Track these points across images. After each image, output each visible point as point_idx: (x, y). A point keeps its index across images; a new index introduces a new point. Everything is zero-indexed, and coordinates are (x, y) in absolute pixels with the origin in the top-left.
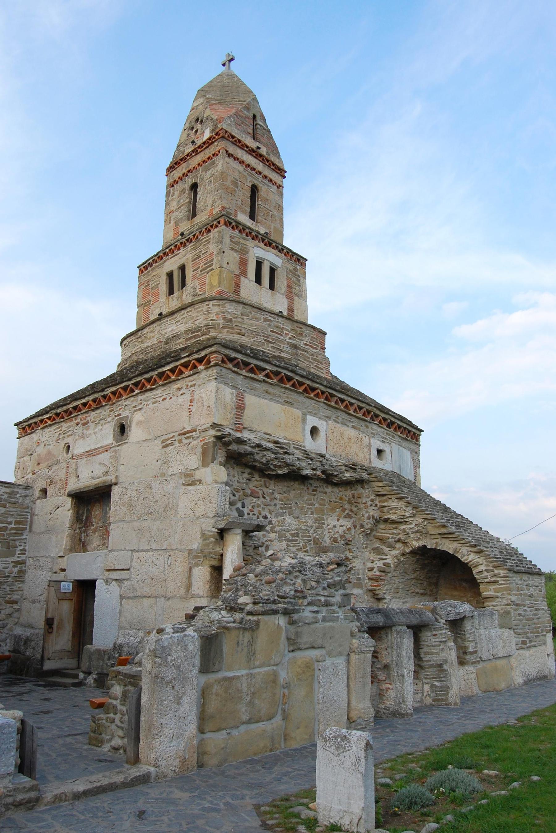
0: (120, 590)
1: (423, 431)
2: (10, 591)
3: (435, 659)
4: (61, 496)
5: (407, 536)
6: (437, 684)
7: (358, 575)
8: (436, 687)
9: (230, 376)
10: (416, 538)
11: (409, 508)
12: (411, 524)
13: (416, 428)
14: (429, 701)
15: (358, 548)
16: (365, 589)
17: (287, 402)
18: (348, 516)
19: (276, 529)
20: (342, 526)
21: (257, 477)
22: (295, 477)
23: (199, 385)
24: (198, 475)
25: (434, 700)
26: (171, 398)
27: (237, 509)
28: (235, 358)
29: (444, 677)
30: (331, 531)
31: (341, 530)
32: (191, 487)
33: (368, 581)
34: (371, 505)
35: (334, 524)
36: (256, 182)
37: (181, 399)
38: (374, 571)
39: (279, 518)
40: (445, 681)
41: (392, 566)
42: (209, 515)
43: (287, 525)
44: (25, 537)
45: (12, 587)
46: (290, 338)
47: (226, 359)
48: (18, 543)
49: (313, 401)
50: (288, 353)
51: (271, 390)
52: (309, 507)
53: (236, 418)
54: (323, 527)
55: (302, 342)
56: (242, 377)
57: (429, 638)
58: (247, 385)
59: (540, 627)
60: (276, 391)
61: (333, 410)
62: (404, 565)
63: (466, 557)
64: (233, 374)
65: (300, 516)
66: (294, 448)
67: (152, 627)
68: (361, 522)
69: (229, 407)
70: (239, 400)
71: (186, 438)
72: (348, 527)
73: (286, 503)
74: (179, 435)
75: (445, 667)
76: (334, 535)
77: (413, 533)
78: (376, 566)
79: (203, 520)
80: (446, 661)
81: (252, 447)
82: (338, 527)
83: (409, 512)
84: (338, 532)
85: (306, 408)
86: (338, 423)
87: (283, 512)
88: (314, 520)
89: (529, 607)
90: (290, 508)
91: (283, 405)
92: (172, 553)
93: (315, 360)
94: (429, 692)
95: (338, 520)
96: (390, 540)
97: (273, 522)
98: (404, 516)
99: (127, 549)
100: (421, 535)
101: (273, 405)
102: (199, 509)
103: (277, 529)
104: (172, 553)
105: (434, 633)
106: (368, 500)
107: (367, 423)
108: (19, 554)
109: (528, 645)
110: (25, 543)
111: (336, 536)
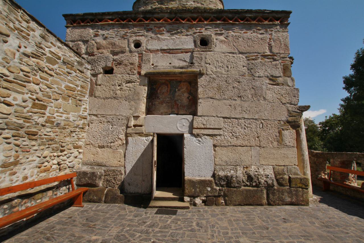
0: (213, 142)
2: (77, 138)
4: (134, 75)
23: (276, 32)
24: (280, 80)
26: (252, 33)
32: (275, 86)
37: (260, 36)
42: (293, 103)
44: (86, 99)
45: (79, 136)
48: (83, 103)
67: (249, 164)
71: (268, 58)
74: (262, 56)
79: (288, 105)
92: (263, 121)
99: (219, 116)
102: (284, 99)
104: (263, 121)
108: (83, 111)
110: (86, 103)
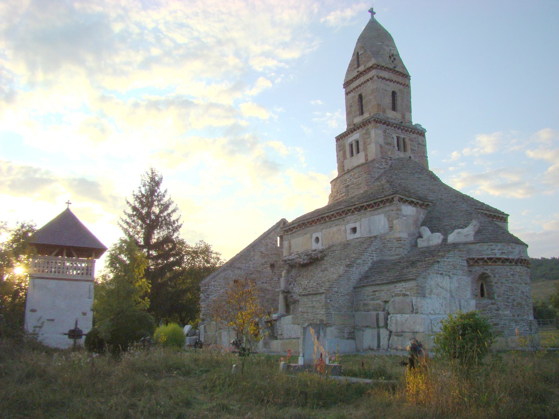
36: (359, 93)
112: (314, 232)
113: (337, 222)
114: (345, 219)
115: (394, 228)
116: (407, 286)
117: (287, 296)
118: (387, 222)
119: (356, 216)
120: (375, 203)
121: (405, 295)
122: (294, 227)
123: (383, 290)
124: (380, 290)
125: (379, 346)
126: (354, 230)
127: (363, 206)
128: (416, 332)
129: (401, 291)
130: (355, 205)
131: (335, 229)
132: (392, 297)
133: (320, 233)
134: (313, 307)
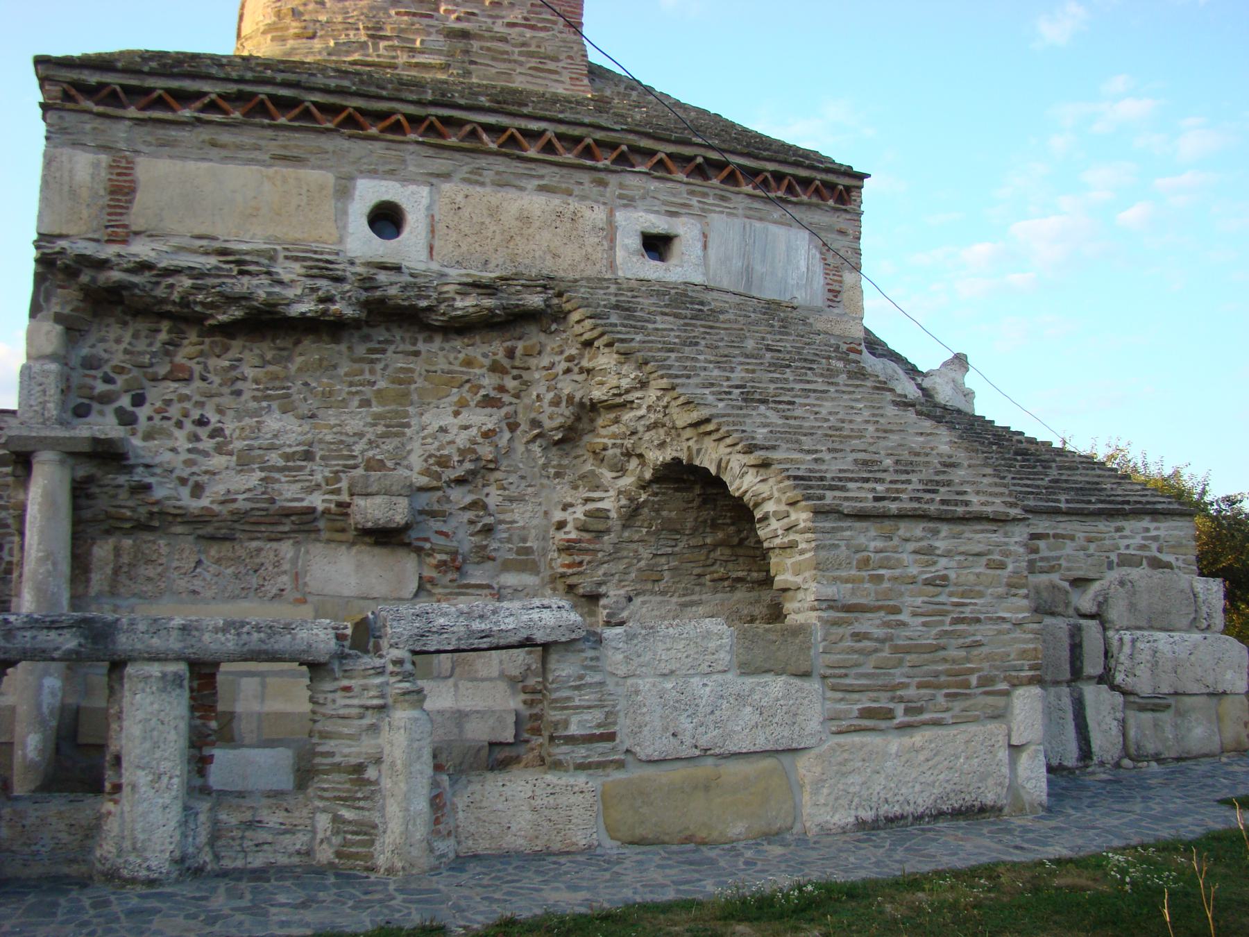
1: (868, 176)
3: (346, 751)
5: (635, 437)
6: (348, 814)
7: (524, 540)
8: (345, 822)
9: (88, 127)
10: (656, 443)
11: (625, 367)
12: (639, 407)
13: (848, 172)
14: (325, 854)
15: (523, 477)
16: (546, 573)
17: (285, 158)
18: (488, 402)
19: (231, 447)
20: (466, 428)
21: (193, 336)
22: (266, 323)
25: (339, 854)
27: (120, 412)
28: (101, 86)
29: (365, 798)
30: (429, 440)
31: (462, 440)
33: (556, 555)
34: (568, 371)
35: (442, 423)
38: (567, 529)
39: (248, 421)
40: (369, 810)
41: (613, 515)
43: (269, 436)
46: (458, 19)
47: (73, 92)
49: (378, 145)
50: (439, 52)
51: (225, 137)
52: (354, 389)
53: (110, 214)
54: (404, 434)
55: (500, 22)
56: (127, 123)
57: (330, 696)
58: (149, 138)
59: (972, 671)
60: (247, 137)
61: (457, 155)
62: (657, 511)
63: (738, 482)
64: (99, 120)
65: (320, 413)
66: (286, 258)
68: (533, 415)
69: (85, 193)
70: (119, 174)
72: (484, 428)
73: (270, 385)
75: (371, 773)
76: (439, 450)
77: (649, 428)
78: (570, 519)
80: (378, 761)
81: (127, 271)
82: (454, 431)
83: (630, 375)
84: (453, 442)
85: (354, 163)
86: (482, 184)
87: (262, 408)
88: (369, 420)
89: (915, 615)
90: (288, 396)
91: (270, 166)
93: (531, 55)
94: (329, 833)
95: (456, 414)
96: (610, 452)
97: (227, 432)
98: (618, 387)
100: (667, 434)
101: (232, 169)
103: (238, 445)
105: (345, 683)
106: (557, 358)
107: (602, 175)
109: (896, 721)
111: (446, 452)
112: (373, 173)
113: (551, 175)
114: (613, 179)
115: (844, 296)
116: (1162, 533)
117: (90, 480)
118: (818, 268)
119: (678, 186)
120: (779, 177)
121: (1156, 564)
122: (184, 98)
123: (1072, 538)
124: (1056, 536)
125: (1086, 753)
126: (657, 245)
127: (725, 164)
128: (1224, 693)
129: (1143, 547)
130: (688, 143)
131: (535, 203)
132: (1110, 566)
133: (425, 191)
134: (940, 582)
